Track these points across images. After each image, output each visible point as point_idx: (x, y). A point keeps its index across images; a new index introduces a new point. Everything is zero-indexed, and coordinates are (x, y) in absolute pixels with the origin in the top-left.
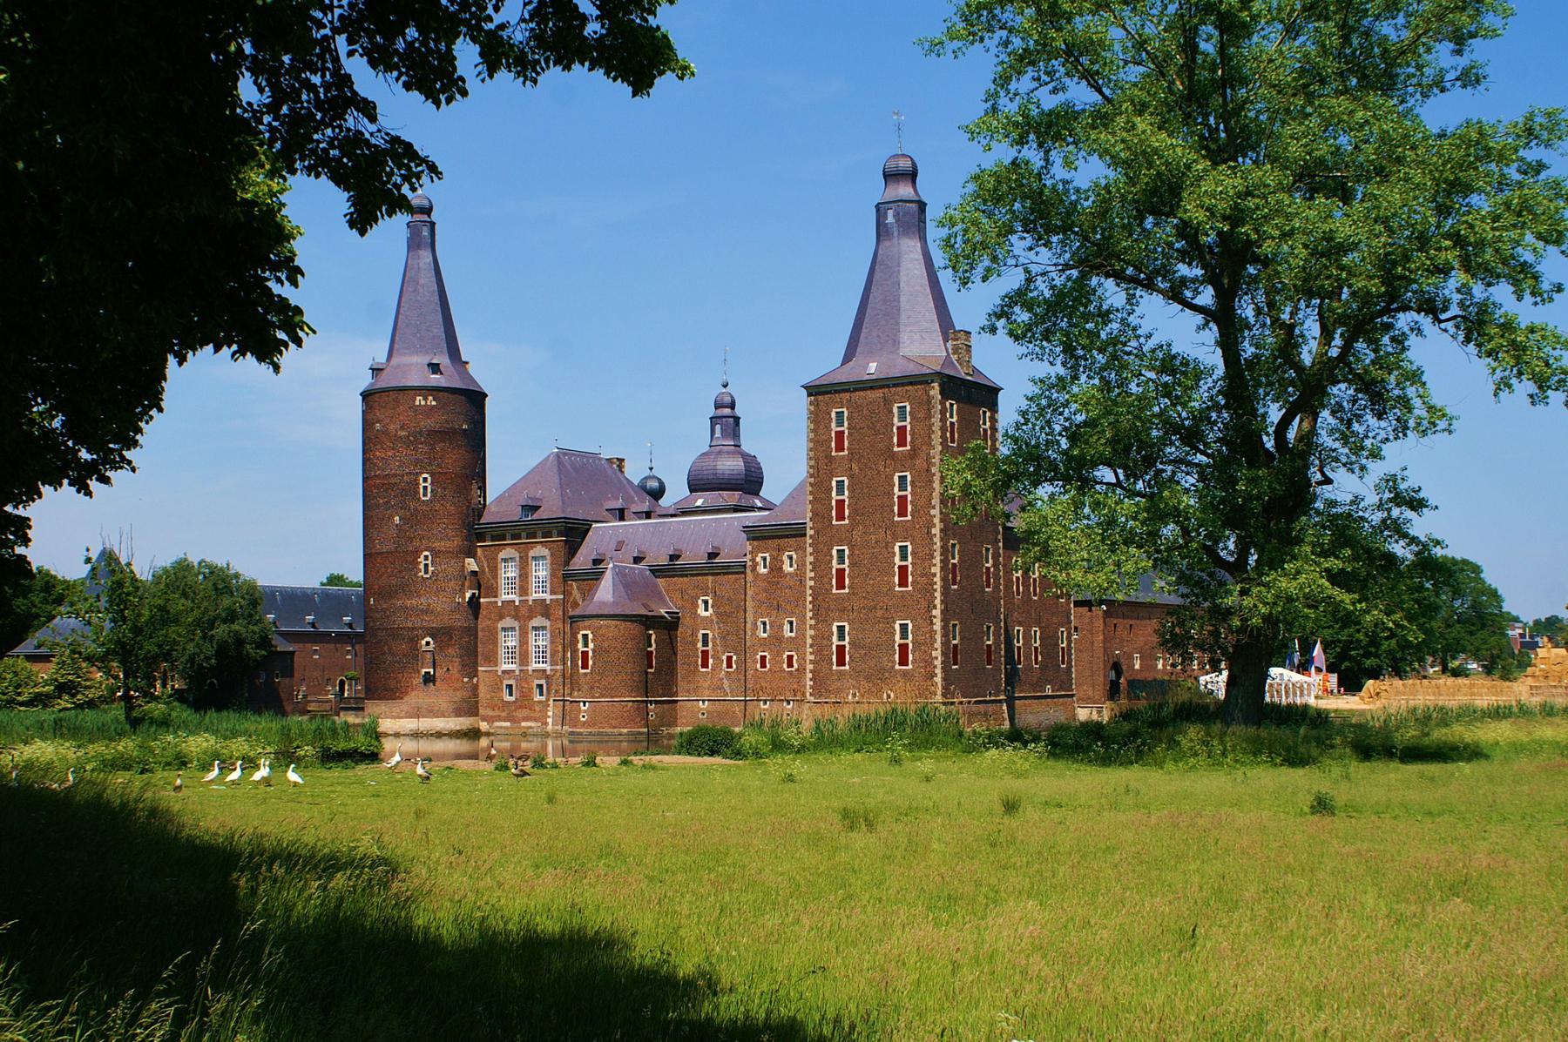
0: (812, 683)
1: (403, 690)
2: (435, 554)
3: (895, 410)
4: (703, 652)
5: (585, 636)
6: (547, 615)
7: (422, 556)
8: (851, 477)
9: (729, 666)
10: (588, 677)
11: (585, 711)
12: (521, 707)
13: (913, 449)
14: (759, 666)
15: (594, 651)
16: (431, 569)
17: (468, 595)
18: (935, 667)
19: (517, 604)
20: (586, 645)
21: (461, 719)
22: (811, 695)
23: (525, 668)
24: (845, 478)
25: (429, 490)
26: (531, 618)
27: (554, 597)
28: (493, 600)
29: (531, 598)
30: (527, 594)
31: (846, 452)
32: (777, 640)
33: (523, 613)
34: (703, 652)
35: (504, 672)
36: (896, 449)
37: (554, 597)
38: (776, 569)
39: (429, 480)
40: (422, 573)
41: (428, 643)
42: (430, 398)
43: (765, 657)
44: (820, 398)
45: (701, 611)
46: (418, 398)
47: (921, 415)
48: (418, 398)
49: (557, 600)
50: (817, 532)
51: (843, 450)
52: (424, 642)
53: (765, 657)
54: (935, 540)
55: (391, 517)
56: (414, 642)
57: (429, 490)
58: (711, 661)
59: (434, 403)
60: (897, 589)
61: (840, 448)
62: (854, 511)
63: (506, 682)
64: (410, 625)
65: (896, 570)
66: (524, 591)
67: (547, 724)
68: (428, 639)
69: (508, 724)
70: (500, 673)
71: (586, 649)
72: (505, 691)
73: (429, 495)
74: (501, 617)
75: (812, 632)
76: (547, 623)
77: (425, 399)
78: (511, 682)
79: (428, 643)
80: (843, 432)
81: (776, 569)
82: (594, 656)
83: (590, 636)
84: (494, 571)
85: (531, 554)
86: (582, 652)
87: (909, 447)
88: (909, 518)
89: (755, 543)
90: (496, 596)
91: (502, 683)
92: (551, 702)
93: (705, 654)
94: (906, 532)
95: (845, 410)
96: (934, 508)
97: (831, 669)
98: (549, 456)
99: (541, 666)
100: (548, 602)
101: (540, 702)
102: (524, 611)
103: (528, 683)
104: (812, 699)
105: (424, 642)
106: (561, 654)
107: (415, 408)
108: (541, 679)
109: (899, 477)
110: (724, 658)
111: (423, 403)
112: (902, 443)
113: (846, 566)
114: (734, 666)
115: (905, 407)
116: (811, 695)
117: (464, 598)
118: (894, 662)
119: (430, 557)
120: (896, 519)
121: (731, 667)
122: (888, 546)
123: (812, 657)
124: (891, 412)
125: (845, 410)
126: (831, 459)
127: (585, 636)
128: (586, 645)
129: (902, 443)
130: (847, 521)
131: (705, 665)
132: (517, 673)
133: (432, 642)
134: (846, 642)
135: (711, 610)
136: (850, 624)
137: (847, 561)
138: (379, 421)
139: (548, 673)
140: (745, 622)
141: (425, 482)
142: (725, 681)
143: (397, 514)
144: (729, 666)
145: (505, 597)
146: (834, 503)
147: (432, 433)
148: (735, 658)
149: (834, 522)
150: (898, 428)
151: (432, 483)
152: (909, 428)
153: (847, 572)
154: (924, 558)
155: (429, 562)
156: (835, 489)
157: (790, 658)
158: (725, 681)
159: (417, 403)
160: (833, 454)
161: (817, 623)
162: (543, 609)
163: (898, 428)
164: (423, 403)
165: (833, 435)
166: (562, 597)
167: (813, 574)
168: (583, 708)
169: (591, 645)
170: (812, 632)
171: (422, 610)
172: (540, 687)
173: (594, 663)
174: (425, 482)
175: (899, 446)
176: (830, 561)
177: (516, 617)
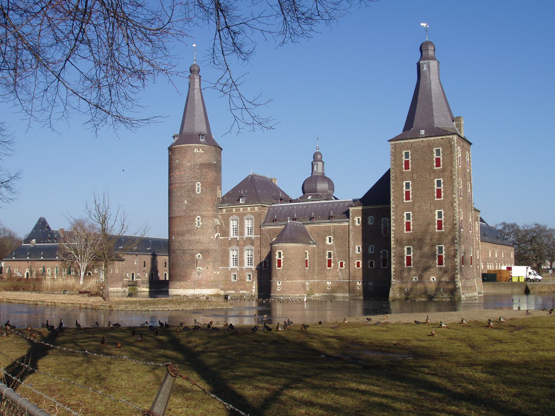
0: (394, 273)
1: (188, 277)
2: (203, 217)
3: (435, 151)
4: (328, 260)
5: (280, 253)
6: (252, 244)
7: (197, 218)
8: (413, 181)
9: (342, 266)
10: (281, 271)
11: (279, 286)
12: (240, 284)
13: (444, 168)
14: (356, 266)
15: (284, 259)
16: (201, 224)
17: (216, 235)
18: (457, 266)
19: (238, 239)
20: (280, 257)
21: (213, 290)
22: (394, 279)
23: (241, 267)
24: (410, 181)
25: (200, 189)
26: (245, 245)
27: (256, 236)
28: (226, 238)
29: (245, 237)
30: (243, 235)
31: (410, 170)
33: (240, 244)
34: (328, 260)
35: (231, 269)
36: (435, 168)
37: (256, 236)
39: (200, 184)
40: (197, 225)
41: (199, 256)
42: (201, 149)
43: (359, 262)
45: (327, 242)
46: (195, 149)
47: (448, 152)
48: (195, 149)
49: (258, 238)
51: (408, 169)
52: (197, 256)
53: (359, 262)
54: (456, 209)
55: (183, 201)
56: (193, 255)
57: (200, 189)
58: (332, 264)
59: (202, 152)
60: (437, 231)
61: (407, 167)
62: (415, 196)
64: (191, 248)
65: (436, 222)
66: (242, 234)
67: (252, 292)
68: (199, 254)
69: (234, 292)
70: (230, 270)
71: (280, 259)
72: (233, 277)
73: (200, 191)
75: (394, 251)
76: (253, 248)
77: (199, 150)
79: (199, 256)
80: (408, 161)
82: (284, 262)
83: (282, 253)
84: (228, 224)
85: (245, 217)
86: (278, 260)
87: (441, 167)
88: (442, 199)
90: (228, 236)
91: (230, 273)
93: (330, 262)
94: (441, 205)
95: (409, 151)
96: (455, 194)
97: (404, 267)
98: (249, 176)
100: (253, 239)
101: (248, 282)
104: (394, 280)
105: (197, 256)
107: (194, 154)
108: (250, 272)
109: (437, 181)
110: (339, 263)
111: (198, 151)
112: (438, 165)
113: (411, 221)
114: (344, 267)
115: (440, 149)
116: (394, 279)
117: (214, 237)
119: (200, 219)
120: (436, 199)
121: (343, 267)
122: (432, 211)
123: (394, 262)
124: (432, 152)
125: (409, 151)
126: (402, 173)
127: (280, 253)
128: (280, 257)
129: (438, 165)
130: (411, 201)
131: (330, 265)
132: (238, 269)
133: (201, 256)
135: (332, 242)
136: (413, 247)
137: (411, 218)
138: (177, 159)
140: (349, 247)
141: (198, 186)
142: (340, 273)
143: (186, 199)
144: (342, 266)
146: (404, 192)
147: (201, 165)
148: (344, 263)
149: (405, 201)
150: (436, 159)
151: (201, 186)
152: (441, 159)
153: (411, 224)
155: (200, 221)
156: (405, 186)
157: (371, 263)
158: (340, 273)
159: (195, 151)
160: (404, 170)
162: (251, 242)
163: (436, 159)
164: (198, 151)
165: (404, 162)
167: (394, 225)
169: (282, 257)
170: (394, 251)
171: (197, 242)
172: (250, 275)
173: (284, 265)
174: (198, 186)
175: (437, 166)
176: (403, 218)
177: (238, 245)
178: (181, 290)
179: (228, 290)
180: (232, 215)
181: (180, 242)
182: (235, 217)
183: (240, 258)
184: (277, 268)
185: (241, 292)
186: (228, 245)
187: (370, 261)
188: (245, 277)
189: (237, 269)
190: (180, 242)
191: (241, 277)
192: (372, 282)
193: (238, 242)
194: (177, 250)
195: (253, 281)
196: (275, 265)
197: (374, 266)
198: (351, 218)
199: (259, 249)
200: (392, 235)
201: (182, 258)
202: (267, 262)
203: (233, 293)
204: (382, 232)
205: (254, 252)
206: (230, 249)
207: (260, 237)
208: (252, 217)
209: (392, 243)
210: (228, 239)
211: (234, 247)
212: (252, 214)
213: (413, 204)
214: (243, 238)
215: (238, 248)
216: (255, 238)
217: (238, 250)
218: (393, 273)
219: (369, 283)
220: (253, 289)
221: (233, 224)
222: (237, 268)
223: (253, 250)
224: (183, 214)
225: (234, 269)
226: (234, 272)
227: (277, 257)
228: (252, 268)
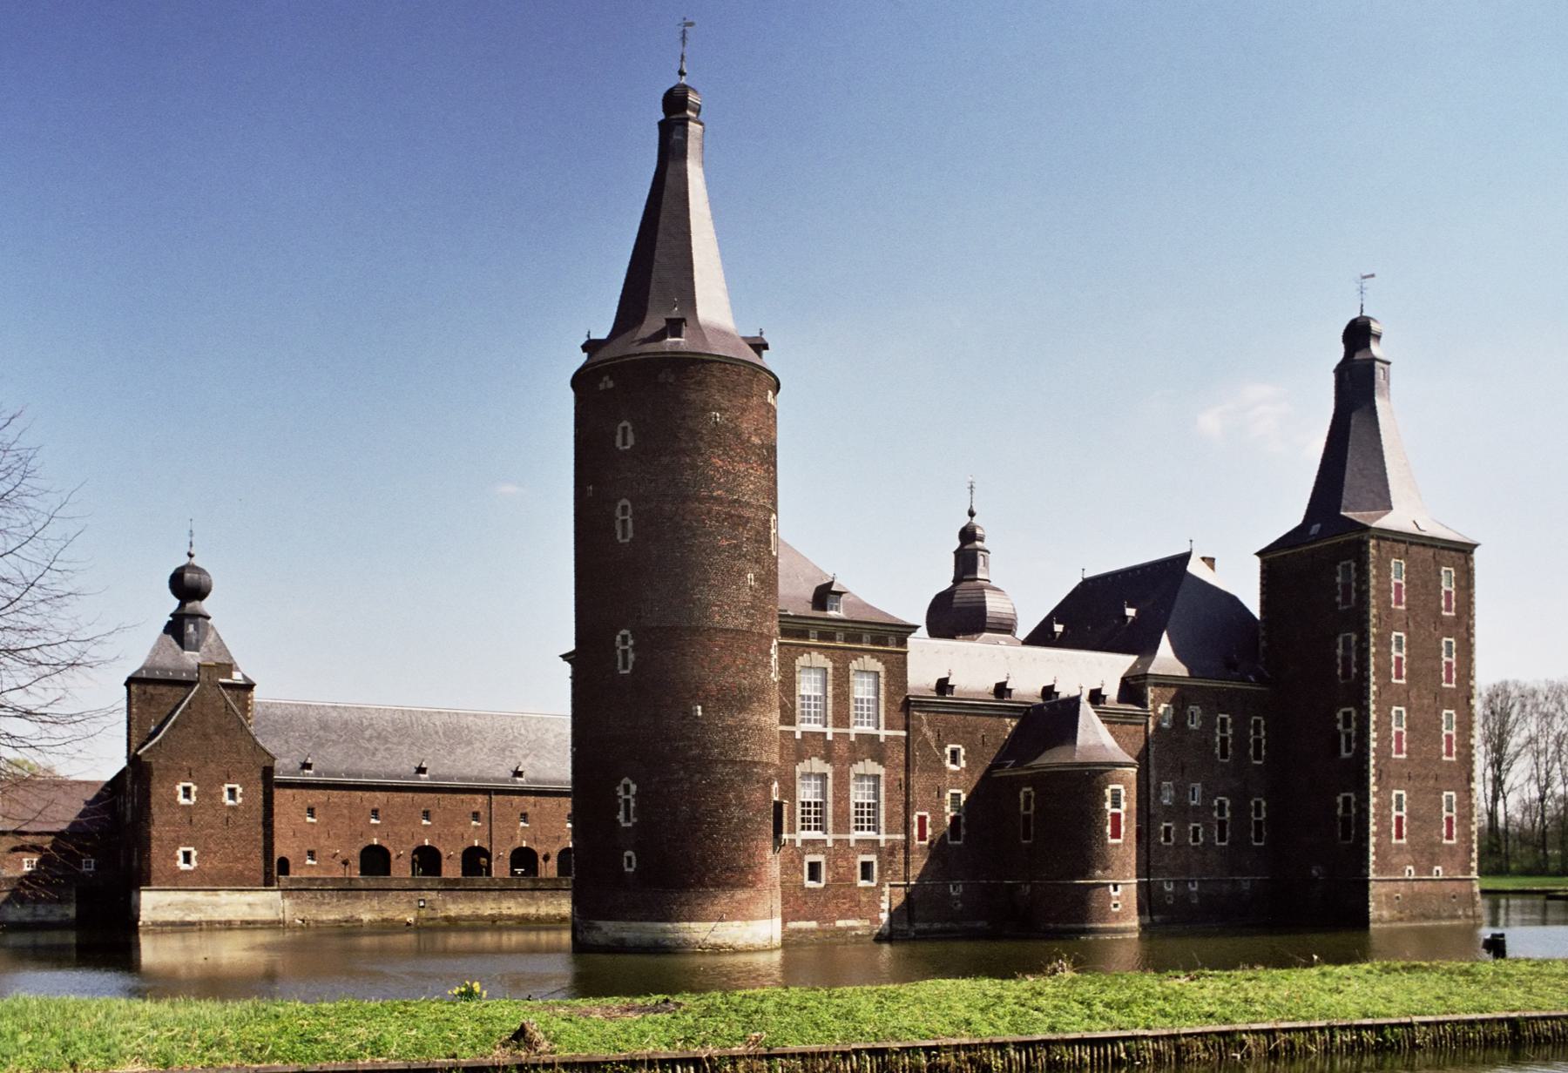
6: (879, 758)
11: (1118, 898)
19: (830, 737)
27: (891, 733)
35: (805, 842)
37: (891, 733)
44: (1382, 544)
49: (896, 738)
50: (1379, 688)
63: (809, 858)
64: (765, 759)
66: (842, 719)
67: (878, 920)
69: (813, 924)
70: (799, 844)
74: (800, 758)
76: (881, 771)
78: (820, 858)
89: (1158, 690)
90: (794, 724)
92: (887, 889)
99: (871, 835)
100: (882, 739)
101: (866, 889)
102: (841, 749)
103: (847, 860)
106: (901, 820)
108: (869, 853)
118: (1441, 835)
132: (830, 844)
134: (1403, 814)
138: (719, 409)
139: (882, 844)
145: (807, 727)
161: (1380, 790)
162: (872, 747)
166: (904, 733)
168: (1114, 894)
173: (1126, 832)
177: (827, 758)
178: (736, 923)
179: (793, 920)
181: (731, 733)
182: (819, 659)
183: (836, 802)
184: (1111, 841)
185: (840, 923)
186: (793, 758)
187: (1164, 824)
188: (852, 869)
189: (824, 841)
190: (730, 729)
191: (841, 870)
192: (1196, 883)
193: (829, 746)
194: (717, 761)
195: (880, 885)
196: (1103, 832)
197: (1201, 839)
198: (1150, 706)
200: (1372, 762)
201: (739, 798)
202: (928, 820)
203: (812, 931)
204: (1217, 751)
205: (887, 787)
207: (907, 738)
208: (879, 667)
209: (1372, 780)
210: (794, 732)
211: (817, 765)
213: (1407, 690)
215: (828, 769)
216: (887, 737)
217: (830, 775)
218: (1372, 858)
219: (1190, 885)
220: (883, 911)
222: (825, 837)
223: (882, 779)
224: (743, 622)
225: (813, 842)
226: (815, 853)
227: (1108, 805)
228: (878, 841)
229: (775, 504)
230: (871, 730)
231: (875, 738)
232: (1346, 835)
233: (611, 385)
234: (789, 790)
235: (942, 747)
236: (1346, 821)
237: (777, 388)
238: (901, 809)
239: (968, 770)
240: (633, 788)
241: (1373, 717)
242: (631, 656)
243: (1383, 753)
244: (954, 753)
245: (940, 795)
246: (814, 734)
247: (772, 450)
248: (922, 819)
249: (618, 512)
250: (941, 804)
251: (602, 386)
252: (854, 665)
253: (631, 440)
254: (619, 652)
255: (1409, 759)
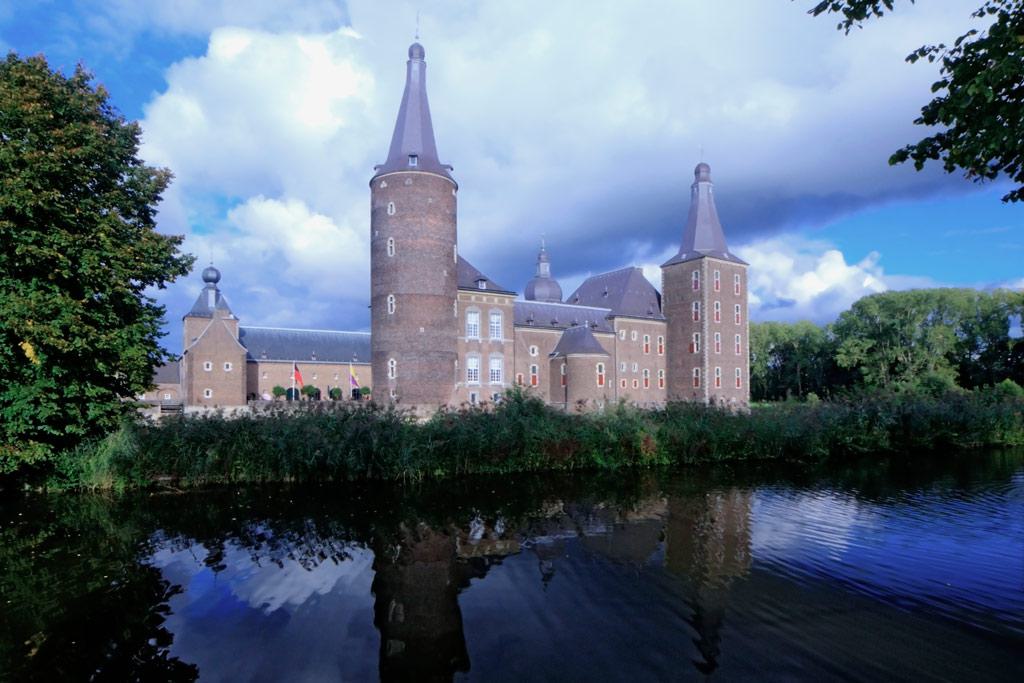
20: (600, 371)
26: (490, 351)
32: (629, 374)
35: (470, 386)
38: (628, 337)
49: (509, 343)
62: (723, 318)
63: (471, 393)
81: (628, 337)
122: (733, 335)
127: (600, 367)
154: (744, 341)
162: (500, 348)
180: (470, 304)
193: (480, 346)
199: (512, 358)
206: (467, 355)
208: (501, 311)
211: (474, 353)
212: (501, 308)
214: (487, 342)
221: (473, 319)
229: (455, 239)
230: (499, 339)
231: (499, 342)
232: (697, 385)
233: (386, 185)
234: (463, 363)
235: (528, 346)
236: (697, 379)
237: (457, 188)
238: (511, 372)
239: (540, 356)
240: (395, 362)
241: (707, 337)
242: (394, 306)
243: (711, 353)
244: (533, 350)
245: (528, 365)
246: (474, 341)
247: (455, 216)
248: (520, 376)
249: (389, 243)
250: (528, 371)
251: (382, 186)
252: (491, 311)
253: (394, 211)
254: (389, 305)
255: (722, 353)
